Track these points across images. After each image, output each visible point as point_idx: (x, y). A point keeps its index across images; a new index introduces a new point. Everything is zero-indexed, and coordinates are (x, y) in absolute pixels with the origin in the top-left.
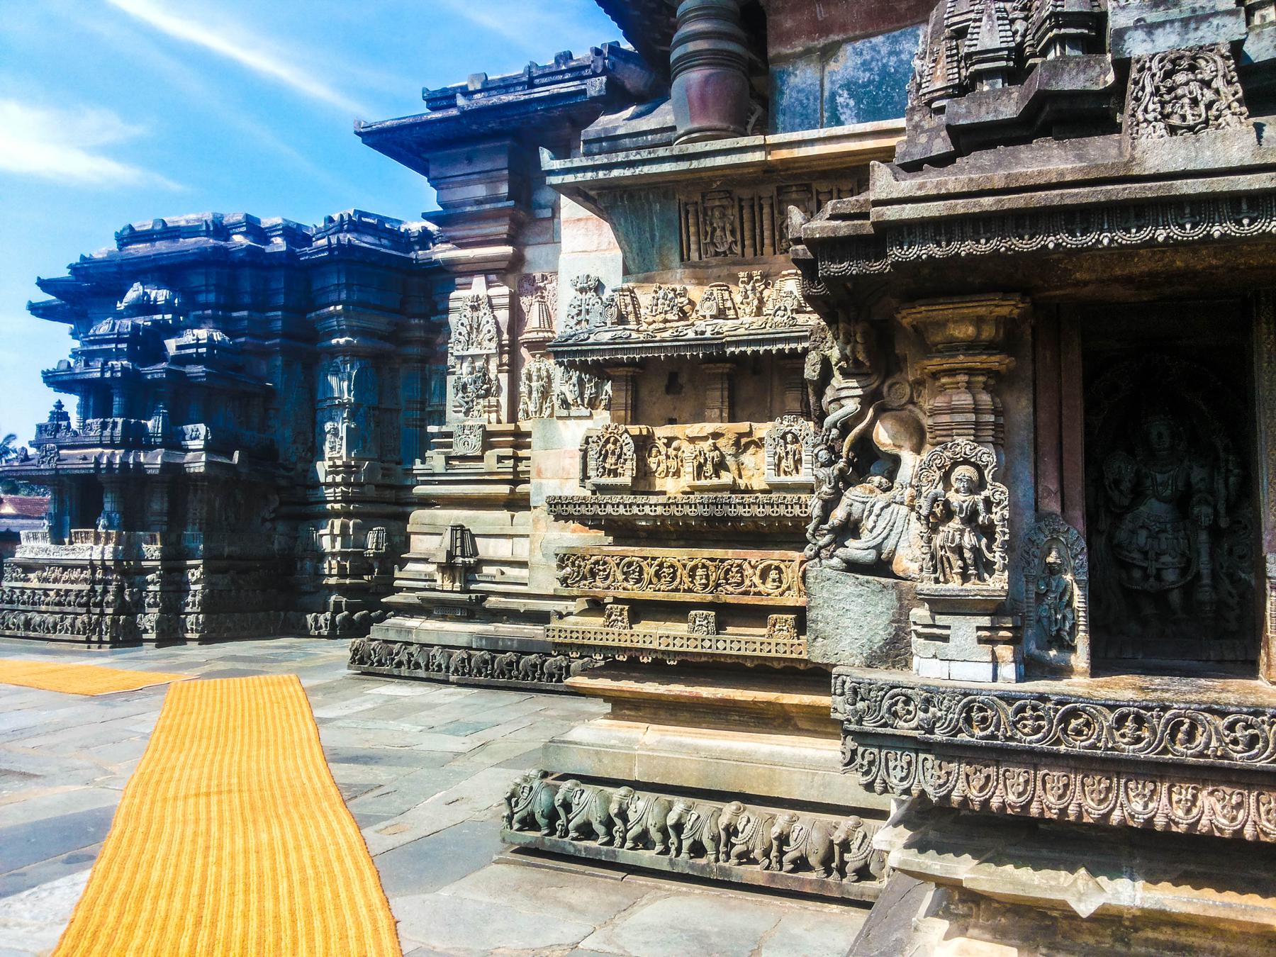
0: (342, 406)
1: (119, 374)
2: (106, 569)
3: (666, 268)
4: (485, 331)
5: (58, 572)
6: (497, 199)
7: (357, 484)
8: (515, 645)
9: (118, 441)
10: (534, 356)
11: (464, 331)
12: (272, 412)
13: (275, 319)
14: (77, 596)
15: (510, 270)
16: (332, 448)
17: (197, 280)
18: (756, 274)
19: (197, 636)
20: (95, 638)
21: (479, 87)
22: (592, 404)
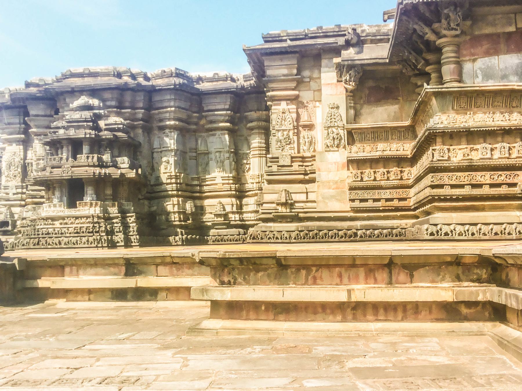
0: (171, 150)
1: (93, 136)
2: (99, 217)
3: (448, 110)
4: (288, 120)
5: (73, 220)
6: (292, 75)
7: (180, 184)
8: (316, 228)
9: (97, 163)
10: (305, 130)
11: (279, 121)
12: (138, 153)
13: (139, 113)
14: (87, 229)
15: (295, 100)
16: (166, 169)
17: (107, 95)
18: (472, 113)
19: (138, 244)
20: (100, 245)
21: (285, 35)
22: (338, 146)
